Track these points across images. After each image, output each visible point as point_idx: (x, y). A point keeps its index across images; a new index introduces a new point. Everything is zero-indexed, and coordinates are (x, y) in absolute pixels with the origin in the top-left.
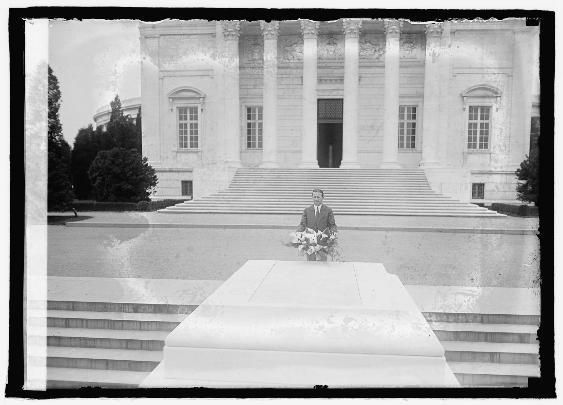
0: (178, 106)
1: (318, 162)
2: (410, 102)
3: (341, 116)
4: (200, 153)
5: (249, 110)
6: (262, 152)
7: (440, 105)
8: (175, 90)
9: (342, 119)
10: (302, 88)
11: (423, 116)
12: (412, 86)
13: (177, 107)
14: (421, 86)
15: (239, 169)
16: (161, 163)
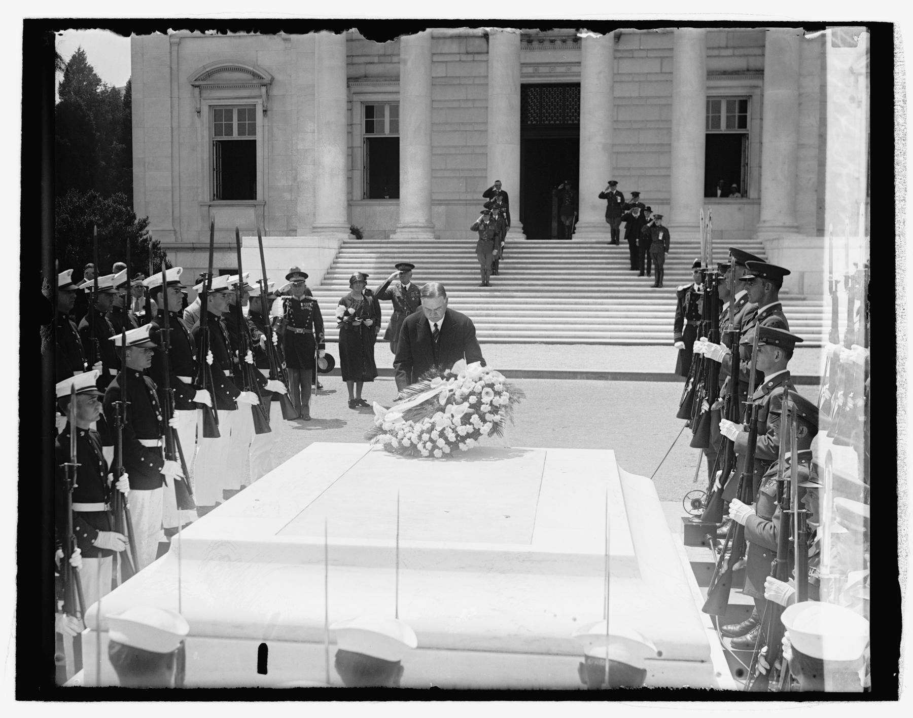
0: (210, 104)
1: (522, 225)
2: (735, 88)
3: (576, 122)
4: (260, 209)
5: (370, 111)
6: (398, 205)
7: (800, 95)
8: (204, 68)
9: (576, 127)
10: (487, 61)
11: (762, 119)
12: (737, 52)
13: (210, 106)
14: (758, 51)
15: (344, 243)
16: (175, 231)
